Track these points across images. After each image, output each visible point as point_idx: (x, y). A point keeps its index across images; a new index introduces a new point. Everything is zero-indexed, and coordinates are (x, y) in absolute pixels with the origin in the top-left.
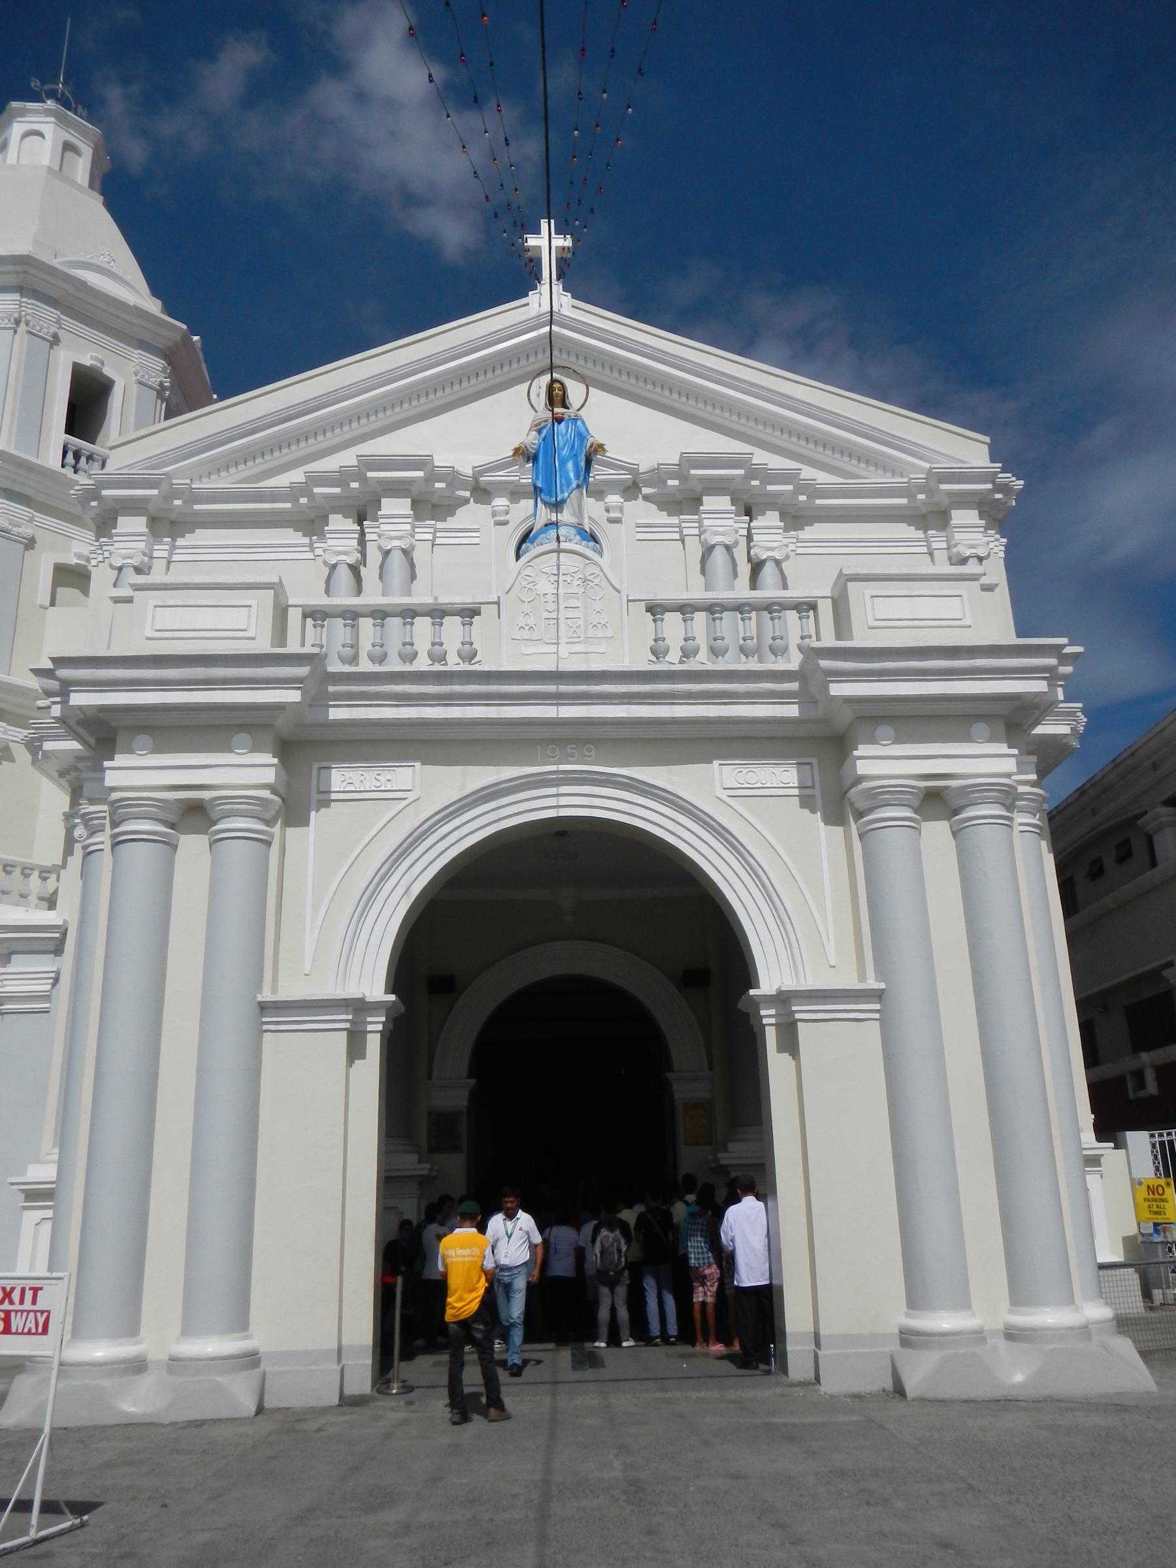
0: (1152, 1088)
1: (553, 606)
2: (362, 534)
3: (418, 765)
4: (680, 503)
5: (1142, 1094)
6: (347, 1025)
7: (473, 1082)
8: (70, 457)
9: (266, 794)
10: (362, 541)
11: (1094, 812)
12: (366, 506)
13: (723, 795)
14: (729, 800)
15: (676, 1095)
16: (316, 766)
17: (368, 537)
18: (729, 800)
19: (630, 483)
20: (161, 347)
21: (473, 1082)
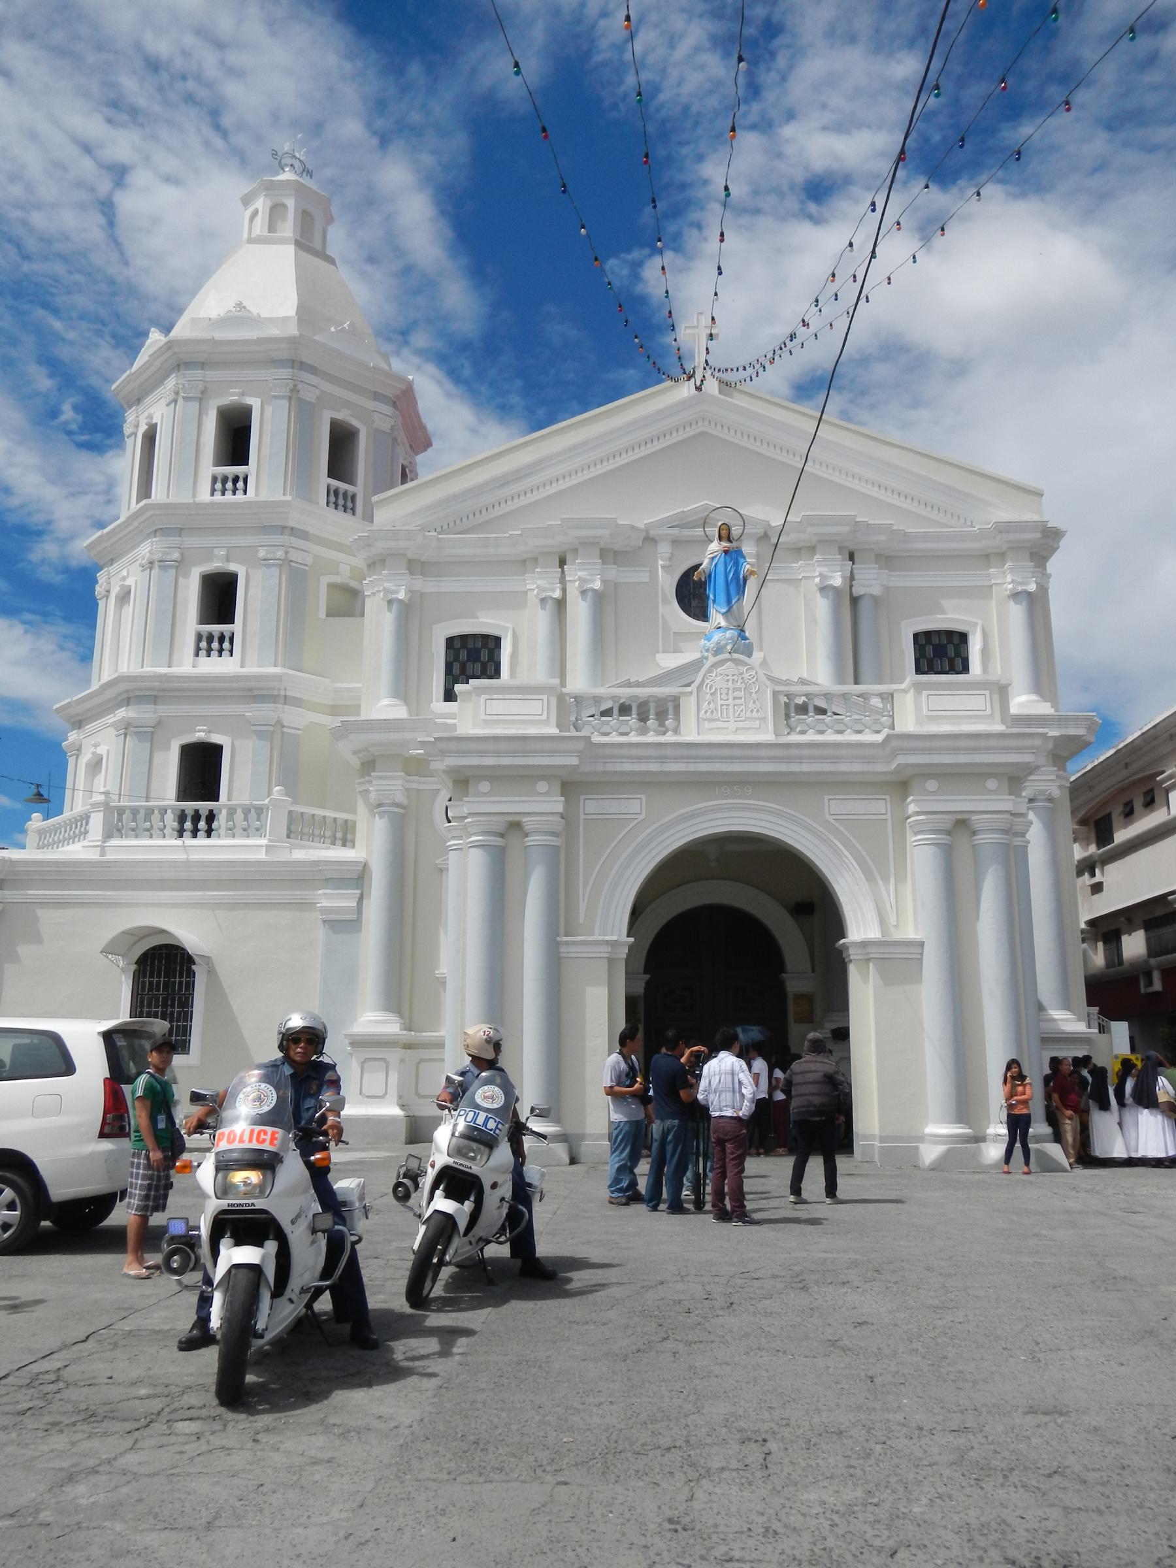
0: (1157, 986)
1: (724, 697)
2: (563, 572)
3: (643, 797)
4: (799, 549)
5: (1150, 990)
6: (608, 955)
7: (648, 976)
8: (332, 499)
9: (558, 818)
10: (563, 580)
11: (1126, 766)
12: (565, 552)
13: (830, 818)
14: (833, 822)
15: (789, 989)
16: (582, 797)
17: (567, 578)
18: (833, 822)
19: (762, 534)
20: (390, 395)
21: (648, 976)
